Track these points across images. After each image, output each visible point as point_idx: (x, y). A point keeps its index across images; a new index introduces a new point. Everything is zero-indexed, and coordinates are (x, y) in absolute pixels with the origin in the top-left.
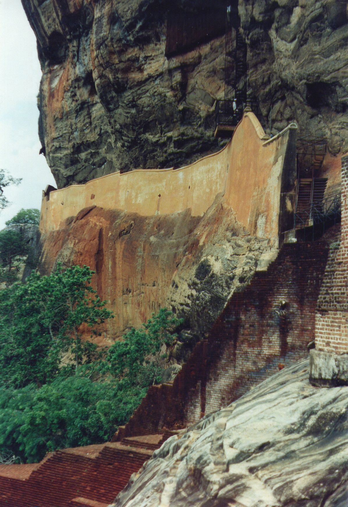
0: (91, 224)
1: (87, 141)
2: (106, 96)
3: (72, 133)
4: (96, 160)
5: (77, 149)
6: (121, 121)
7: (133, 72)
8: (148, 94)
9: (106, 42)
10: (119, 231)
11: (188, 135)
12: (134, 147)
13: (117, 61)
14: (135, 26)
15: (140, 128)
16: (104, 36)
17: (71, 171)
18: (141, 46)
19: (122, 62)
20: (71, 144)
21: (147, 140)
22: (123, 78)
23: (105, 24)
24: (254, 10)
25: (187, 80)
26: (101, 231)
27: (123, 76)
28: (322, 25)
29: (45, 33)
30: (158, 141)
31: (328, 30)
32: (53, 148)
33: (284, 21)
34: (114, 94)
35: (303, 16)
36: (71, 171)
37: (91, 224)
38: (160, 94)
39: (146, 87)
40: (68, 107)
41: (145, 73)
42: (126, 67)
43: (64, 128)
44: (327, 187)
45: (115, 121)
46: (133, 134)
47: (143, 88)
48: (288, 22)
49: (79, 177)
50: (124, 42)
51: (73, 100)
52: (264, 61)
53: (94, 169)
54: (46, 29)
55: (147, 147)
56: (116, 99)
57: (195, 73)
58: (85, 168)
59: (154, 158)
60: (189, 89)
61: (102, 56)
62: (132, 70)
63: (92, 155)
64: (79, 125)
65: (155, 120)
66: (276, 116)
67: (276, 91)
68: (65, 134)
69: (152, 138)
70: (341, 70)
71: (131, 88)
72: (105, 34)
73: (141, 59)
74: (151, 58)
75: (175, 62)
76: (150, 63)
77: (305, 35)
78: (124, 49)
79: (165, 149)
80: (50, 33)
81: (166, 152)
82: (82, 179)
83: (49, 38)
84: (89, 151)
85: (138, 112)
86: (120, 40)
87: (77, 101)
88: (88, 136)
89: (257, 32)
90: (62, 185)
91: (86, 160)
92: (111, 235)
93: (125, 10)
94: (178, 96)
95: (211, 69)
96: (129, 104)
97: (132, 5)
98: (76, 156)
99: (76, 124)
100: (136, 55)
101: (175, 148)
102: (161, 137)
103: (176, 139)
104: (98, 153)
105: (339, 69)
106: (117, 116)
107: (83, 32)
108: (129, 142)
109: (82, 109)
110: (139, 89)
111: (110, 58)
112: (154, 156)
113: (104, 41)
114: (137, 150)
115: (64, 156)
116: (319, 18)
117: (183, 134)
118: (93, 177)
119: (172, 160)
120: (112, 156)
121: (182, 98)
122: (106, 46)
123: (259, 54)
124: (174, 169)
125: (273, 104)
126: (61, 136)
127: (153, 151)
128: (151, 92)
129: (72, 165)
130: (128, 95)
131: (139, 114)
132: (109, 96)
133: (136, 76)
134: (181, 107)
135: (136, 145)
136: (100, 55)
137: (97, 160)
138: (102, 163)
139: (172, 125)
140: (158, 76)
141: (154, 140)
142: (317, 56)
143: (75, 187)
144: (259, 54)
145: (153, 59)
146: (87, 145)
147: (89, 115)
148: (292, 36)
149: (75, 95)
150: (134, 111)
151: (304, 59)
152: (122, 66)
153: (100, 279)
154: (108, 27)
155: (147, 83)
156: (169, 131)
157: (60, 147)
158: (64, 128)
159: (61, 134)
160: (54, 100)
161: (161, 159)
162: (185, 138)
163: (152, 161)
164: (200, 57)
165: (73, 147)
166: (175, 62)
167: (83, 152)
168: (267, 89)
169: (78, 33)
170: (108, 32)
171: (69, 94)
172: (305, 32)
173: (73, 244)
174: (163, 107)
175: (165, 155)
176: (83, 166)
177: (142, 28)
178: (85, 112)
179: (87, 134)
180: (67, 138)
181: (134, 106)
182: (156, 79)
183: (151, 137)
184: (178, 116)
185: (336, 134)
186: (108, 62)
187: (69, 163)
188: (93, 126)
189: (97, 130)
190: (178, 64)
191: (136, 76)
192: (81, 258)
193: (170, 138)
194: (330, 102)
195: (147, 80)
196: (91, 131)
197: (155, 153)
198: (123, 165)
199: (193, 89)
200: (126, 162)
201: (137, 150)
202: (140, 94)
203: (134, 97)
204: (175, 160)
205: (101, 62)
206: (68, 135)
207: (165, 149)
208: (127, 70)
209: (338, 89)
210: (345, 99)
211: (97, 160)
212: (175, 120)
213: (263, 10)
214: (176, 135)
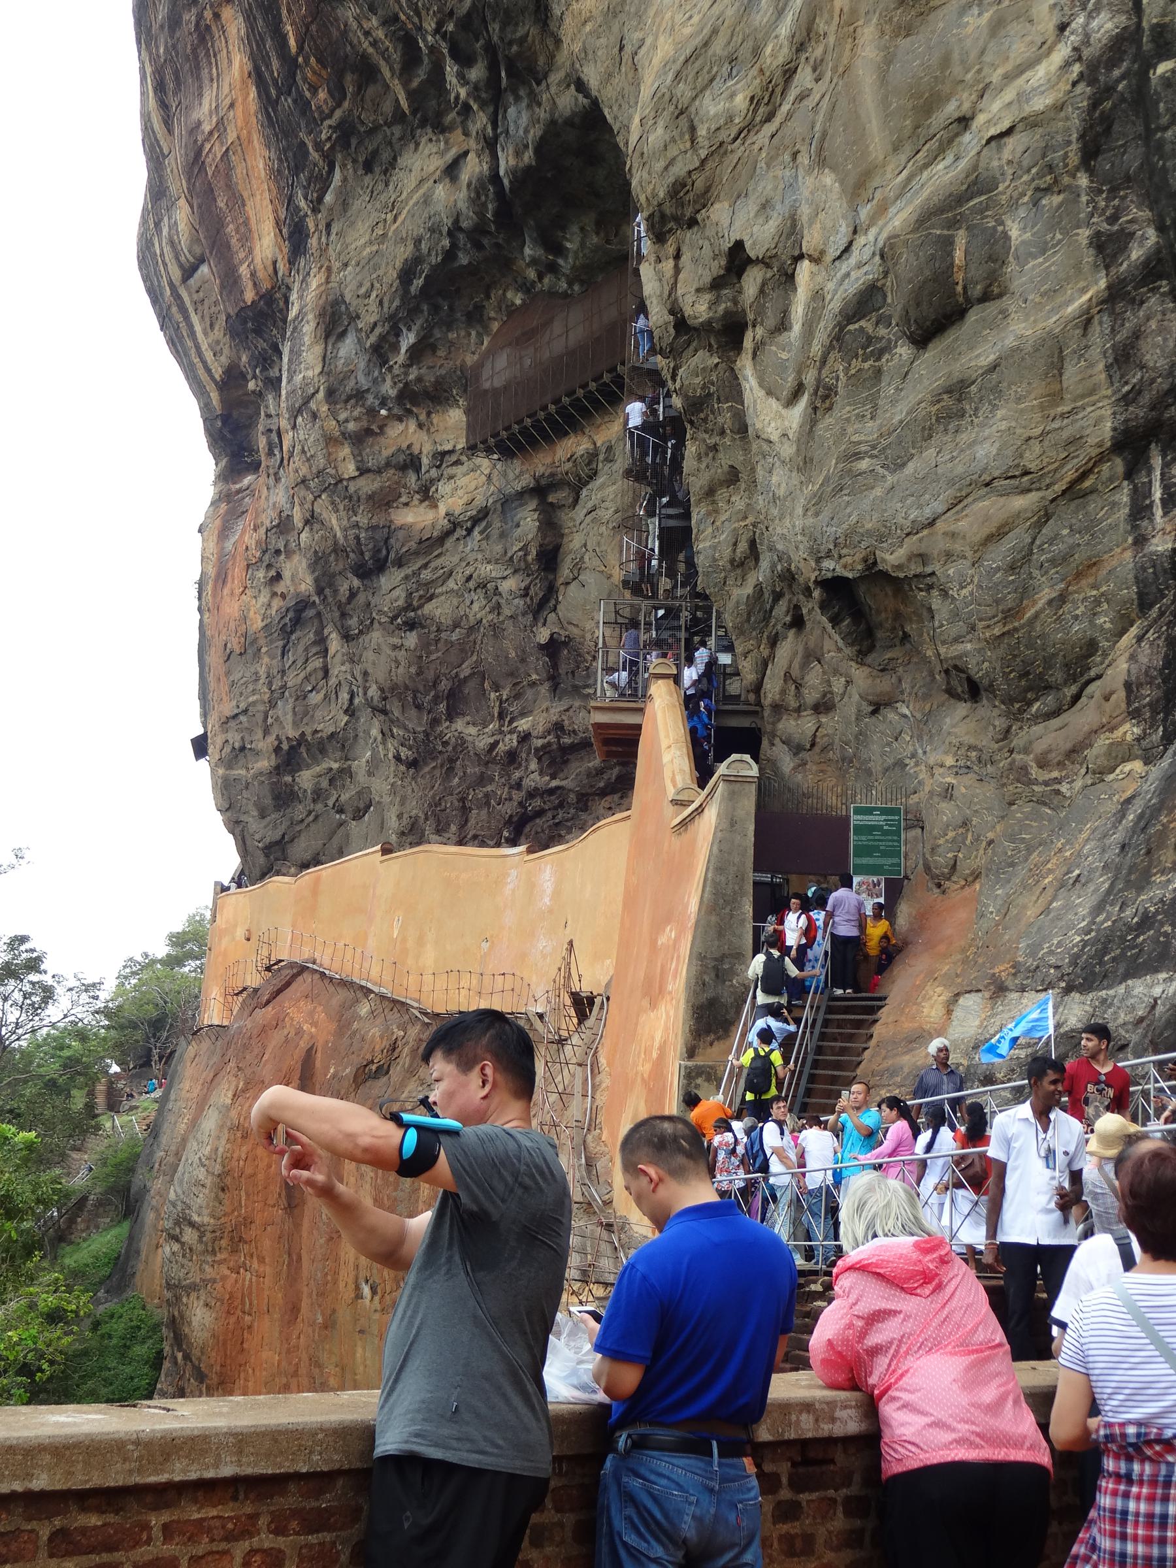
0: (288, 1030)
1: (316, 732)
2: (331, 585)
3: (272, 704)
4: (344, 797)
5: (290, 758)
6: (380, 673)
7: (406, 504)
8: (451, 584)
9: (313, 405)
10: (357, 1061)
11: (574, 731)
12: (426, 764)
13: (350, 469)
14: (395, 347)
15: (436, 700)
16: (306, 383)
17: (275, 827)
18: (423, 417)
19: (368, 471)
20: (271, 739)
21: (462, 742)
22: (373, 528)
23: (307, 339)
24: (681, 276)
25: (562, 536)
26: (310, 1054)
27: (374, 521)
28: (882, 331)
29: (208, 371)
30: (494, 745)
31: (904, 351)
32: (227, 749)
33: (771, 321)
34: (356, 583)
35: (818, 296)
36: (275, 827)
37: (288, 1030)
38: (482, 586)
39: (449, 559)
40: (259, 618)
41: (442, 509)
42: (382, 488)
43: (251, 687)
44: (873, 1043)
45: (366, 674)
46: (420, 718)
47: (438, 562)
48: (783, 326)
49: (301, 848)
51: (274, 594)
52: (733, 477)
53: (341, 824)
55: (464, 767)
56: (361, 598)
57: (580, 512)
58: (317, 817)
59: (488, 804)
60: (565, 572)
61: (303, 451)
62: (404, 499)
64: (293, 679)
65: (480, 674)
66: (783, 692)
67: (777, 597)
68: (254, 703)
69: (473, 733)
70: (940, 525)
71: (399, 563)
72: (310, 373)
73: (425, 461)
74: (454, 458)
75: (519, 474)
76: (451, 477)
77: (824, 373)
78: (374, 427)
79: (517, 774)
80: (220, 370)
81: (518, 786)
82: (307, 856)
84: (325, 765)
85: (426, 645)
86: (359, 395)
87: (283, 596)
88: (318, 714)
89: (699, 363)
90: (257, 872)
91: (318, 795)
92: (334, 1076)
93: (363, 291)
94: (532, 592)
96: (395, 618)
97: (380, 272)
98: (288, 779)
99: (283, 672)
100: (409, 447)
101: (541, 774)
102: (501, 732)
103: (539, 743)
104: (345, 772)
105: (932, 523)
106: (369, 655)
108: (410, 748)
109: (297, 622)
110: (425, 566)
111: (330, 460)
112: (487, 795)
113: (306, 402)
114: (437, 773)
115: (255, 777)
116: (867, 301)
117: (558, 727)
118: (341, 853)
119: (540, 813)
120: (380, 787)
121: (543, 602)
122: (314, 416)
123: (715, 448)
124: (530, 851)
125: (774, 642)
126: (245, 711)
127: (482, 780)
128: (460, 578)
129: (278, 808)
130: (391, 588)
131: (429, 653)
133: (415, 518)
134: (543, 635)
135: (433, 759)
136: (298, 448)
138: (362, 806)
139: (529, 694)
140: (476, 521)
141: (483, 743)
142: (864, 464)
143: (278, 883)
144: (715, 448)
145: (458, 463)
146: (321, 747)
147: (321, 641)
148: (790, 381)
149: (278, 577)
150: (412, 639)
151: (824, 473)
152: (367, 485)
153: (297, 1226)
154: (318, 349)
155: (449, 543)
156: (523, 714)
157: (243, 748)
158: (251, 687)
159: (243, 706)
160: (226, 591)
161: (509, 809)
162: (567, 740)
163: (484, 812)
164: (593, 456)
165: (277, 750)
166: (519, 474)
167: (308, 767)
168: (748, 589)
170: (318, 370)
171: (261, 574)
172: (824, 362)
173: (230, 1094)
175: (517, 796)
176: (310, 812)
177: (416, 354)
178: (308, 635)
179: (317, 706)
180: (260, 717)
181: (411, 625)
182: (469, 531)
183: (473, 730)
185: (948, 793)
186: (319, 473)
187: (268, 801)
188: (333, 681)
189: (344, 696)
190: (526, 481)
191: (415, 518)
192: (244, 1148)
193: (525, 737)
194: (929, 653)
195: (448, 534)
196: (326, 696)
197: (489, 788)
198: (405, 821)
199: (578, 567)
200: (413, 813)
201: (437, 773)
202: (428, 584)
203: (410, 595)
204: (550, 814)
205: (304, 471)
206: (261, 708)
207: (517, 774)
208: (384, 501)
209: (936, 602)
210: (960, 648)
212: (534, 677)
213: (707, 279)
214: (541, 729)
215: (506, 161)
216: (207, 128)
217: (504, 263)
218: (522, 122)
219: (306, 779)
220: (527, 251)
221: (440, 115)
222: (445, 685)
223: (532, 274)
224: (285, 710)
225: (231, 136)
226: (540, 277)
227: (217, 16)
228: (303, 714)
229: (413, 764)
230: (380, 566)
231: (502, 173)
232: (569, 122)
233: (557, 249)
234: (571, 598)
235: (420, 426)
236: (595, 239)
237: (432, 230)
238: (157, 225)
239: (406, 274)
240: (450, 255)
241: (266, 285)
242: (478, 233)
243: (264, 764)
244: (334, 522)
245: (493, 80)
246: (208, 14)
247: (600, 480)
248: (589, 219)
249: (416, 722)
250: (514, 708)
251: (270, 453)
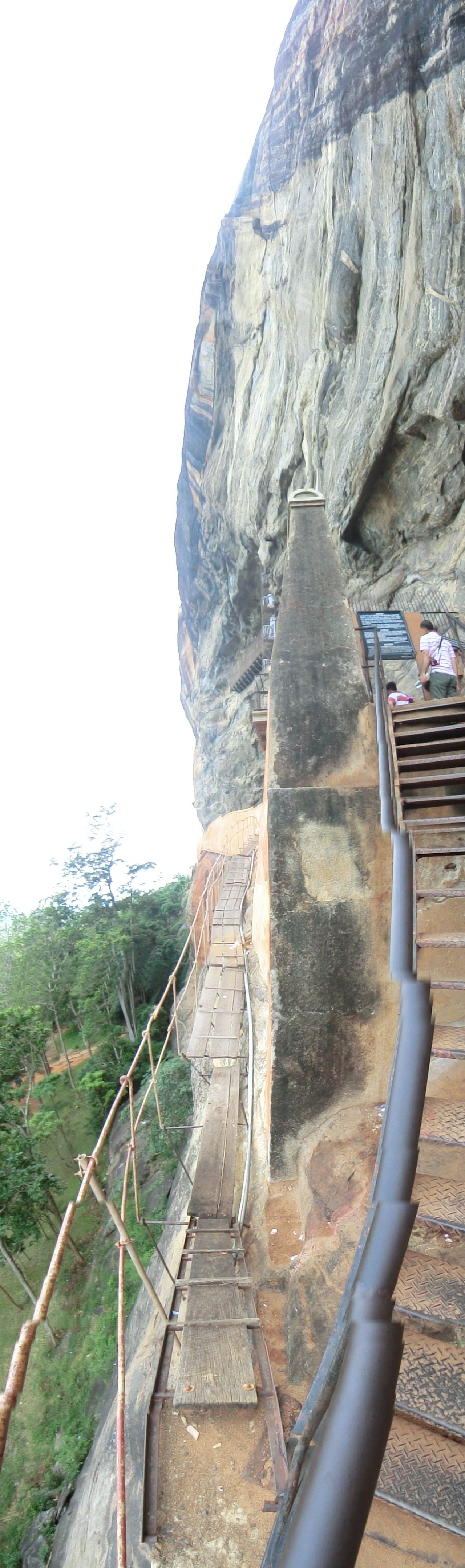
5: (208, 803)
6: (218, 769)
21: (237, 784)
50: (211, 692)
63: (218, 805)
64: (207, 782)
69: (239, 780)
85: (227, 757)
86: (208, 692)
91: (215, 811)
104: (220, 804)
127: (243, 793)
132: (209, 748)
137: (220, 809)
141: (242, 782)
150: (224, 757)
152: (210, 716)
161: (251, 801)
174: (242, 747)
175: (252, 795)
178: (209, 771)
181: (223, 752)
184: (253, 751)
195: (230, 723)
208: (215, 719)
211: (220, 809)
215: (232, 595)
217: (237, 639)
218: (233, 579)
219: (212, 807)
222: (232, 768)
223: (244, 639)
224: (205, 789)
226: (246, 638)
228: (209, 790)
229: (227, 793)
230: (215, 737)
232: (244, 569)
233: (248, 623)
239: (214, 652)
240: (224, 641)
243: (203, 805)
244: (204, 727)
245: (225, 571)
249: (226, 781)
250: (249, 770)
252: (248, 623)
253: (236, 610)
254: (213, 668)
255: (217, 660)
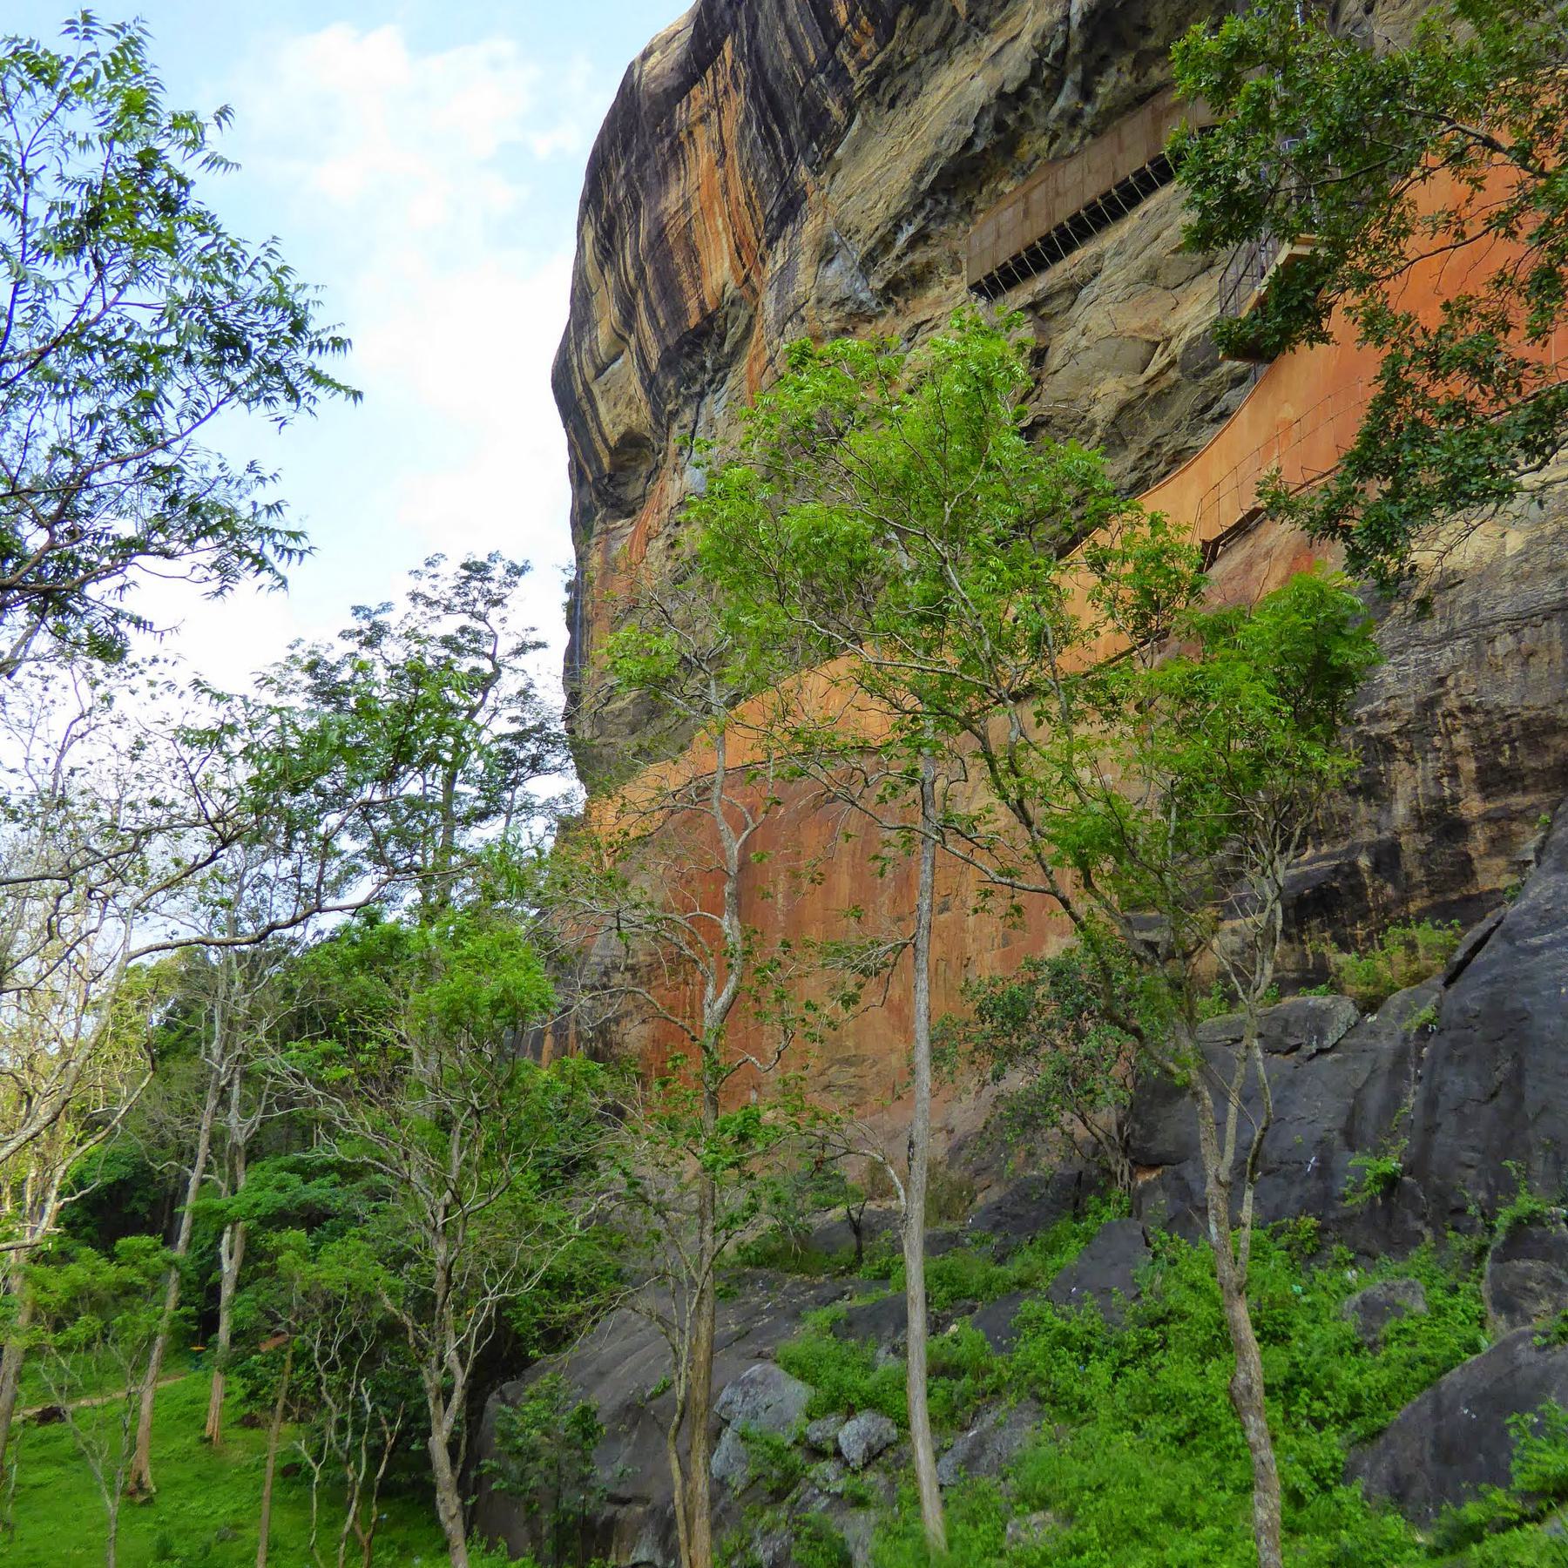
9: (803, 312)
18: (901, 304)
29: (605, 440)
54: (607, 429)
60: (1055, 360)
83: (614, 452)
86: (841, 303)
95: (1143, 271)
107: (711, 382)
113: (797, 310)
154: (812, 270)
169: (696, 388)
171: (660, 543)
216: (673, 210)
220: (1061, 102)
221: (988, 19)
225: (695, 208)
227: (690, 134)
231: (1073, 10)
233: (1087, 94)
234: (1054, 388)
235: (898, 312)
236: (1128, 79)
237: (959, 122)
238: (578, 345)
239: (921, 173)
240: (969, 143)
241: (710, 309)
242: (1021, 94)
246: (683, 135)
247: (1103, 276)
248: (1127, 60)
251: (680, 454)
252: (1087, 94)
253: (1075, 48)
254: (898, 228)
255: (920, 206)
